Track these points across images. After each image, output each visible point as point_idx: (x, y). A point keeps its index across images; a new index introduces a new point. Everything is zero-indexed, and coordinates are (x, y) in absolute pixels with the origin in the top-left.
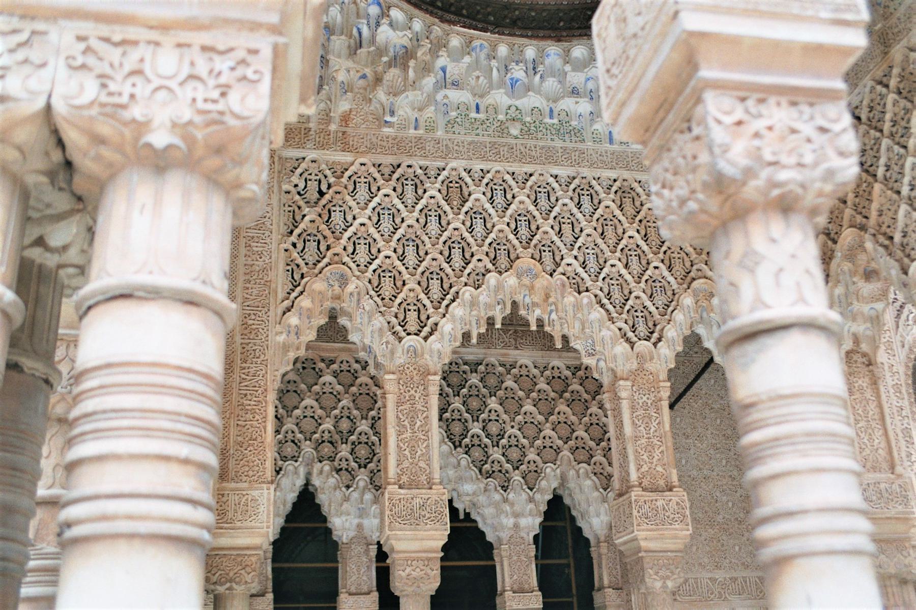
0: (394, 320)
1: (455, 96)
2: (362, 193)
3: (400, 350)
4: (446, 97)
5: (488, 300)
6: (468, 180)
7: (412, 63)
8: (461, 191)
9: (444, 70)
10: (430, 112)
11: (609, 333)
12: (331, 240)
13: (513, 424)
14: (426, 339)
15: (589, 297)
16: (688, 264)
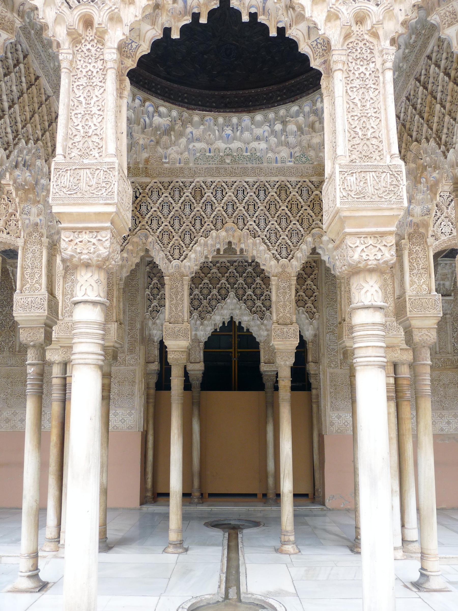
0: (168, 253)
1: (199, 145)
2: (155, 196)
3: (171, 266)
4: (194, 146)
5: (212, 243)
6: (204, 187)
7: (172, 133)
8: (201, 192)
9: (192, 133)
10: (186, 154)
11: (268, 256)
12: (141, 219)
13: (267, 289)
14: (182, 261)
15: (259, 240)
16: (311, 221)
